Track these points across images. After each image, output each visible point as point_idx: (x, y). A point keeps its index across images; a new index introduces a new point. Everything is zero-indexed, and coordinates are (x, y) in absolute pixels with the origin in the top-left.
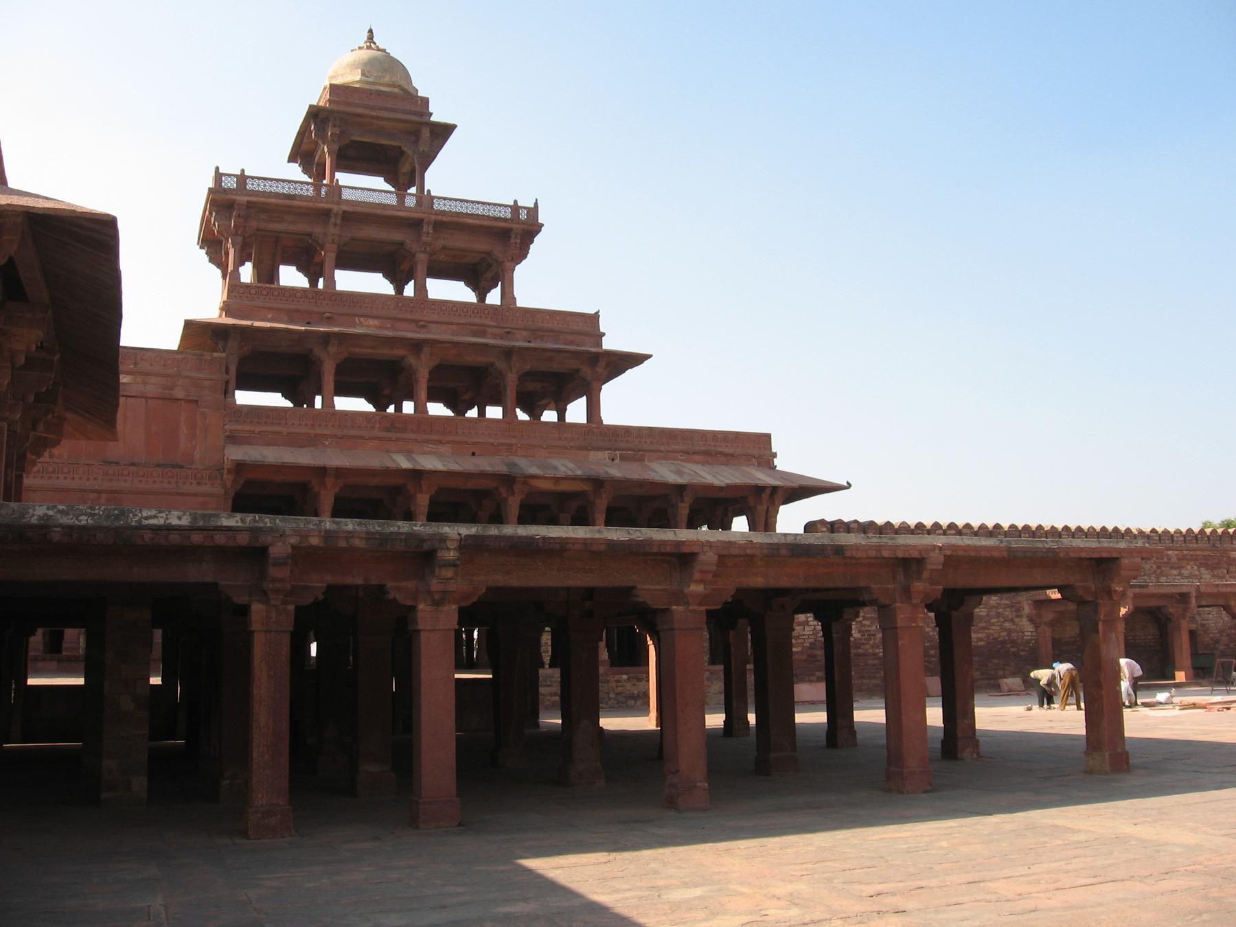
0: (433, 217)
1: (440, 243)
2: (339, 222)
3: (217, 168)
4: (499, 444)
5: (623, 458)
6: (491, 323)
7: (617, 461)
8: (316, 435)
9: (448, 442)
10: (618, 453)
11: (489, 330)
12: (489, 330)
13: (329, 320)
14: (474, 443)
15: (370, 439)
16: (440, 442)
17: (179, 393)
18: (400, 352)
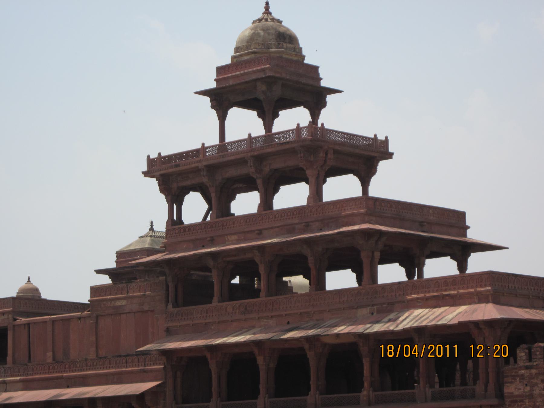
0: (249, 154)
1: (267, 169)
2: (205, 173)
3: (149, 156)
4: (301, 313)
5: (379, 312)
6: (296, 221)
7: (375, 314)
8: (206, 323)
9: (272, 317)
10: (375, 307)
11: (297, 227)
12: (297, 227)
13: (212, 242)
14: (286, 315)
15: (232, 321)
16: (267, 318)
17: (146, 308)
18: (249, 256)
